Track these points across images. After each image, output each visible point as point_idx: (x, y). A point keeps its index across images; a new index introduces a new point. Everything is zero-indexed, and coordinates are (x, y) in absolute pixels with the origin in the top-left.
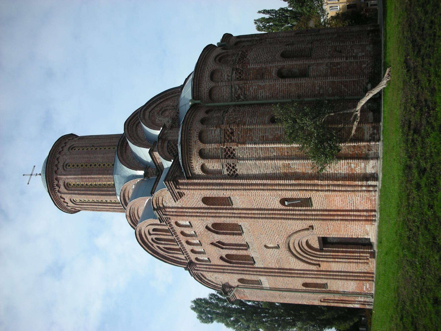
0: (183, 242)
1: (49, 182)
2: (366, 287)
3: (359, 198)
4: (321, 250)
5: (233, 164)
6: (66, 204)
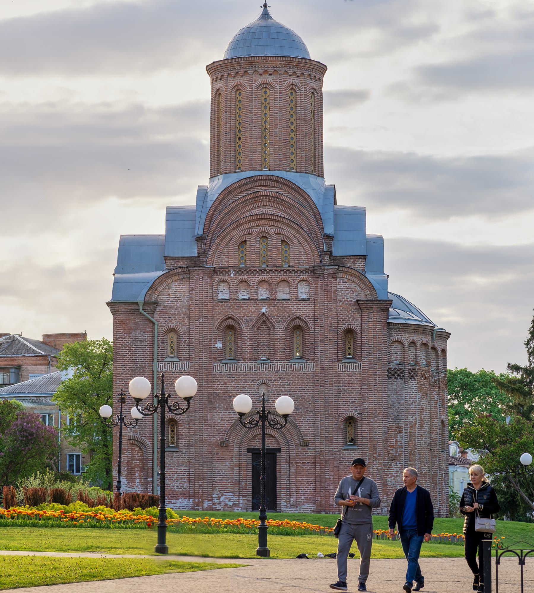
0: (265, 277)
1: (301, 63)
4: (249, 450)
5: (403, 376)
6: (261, 71)
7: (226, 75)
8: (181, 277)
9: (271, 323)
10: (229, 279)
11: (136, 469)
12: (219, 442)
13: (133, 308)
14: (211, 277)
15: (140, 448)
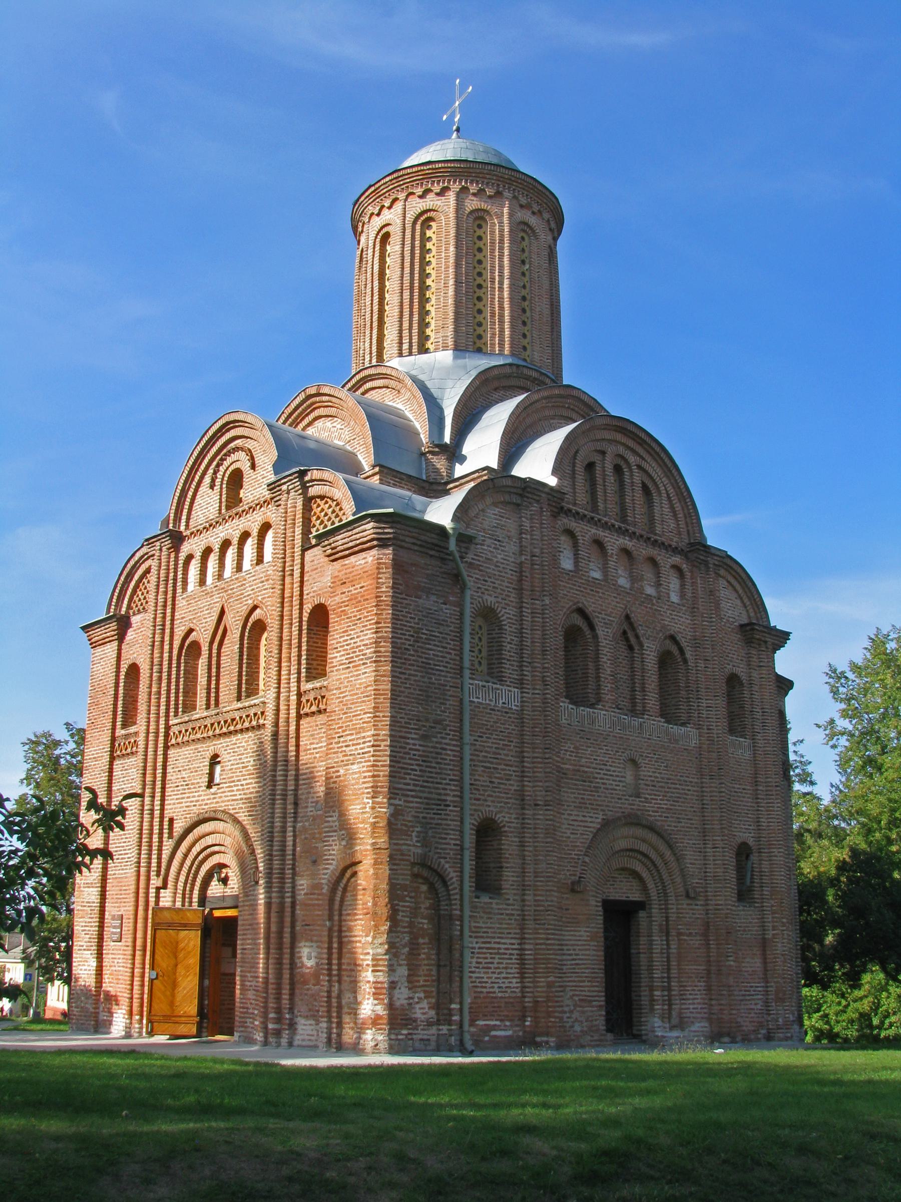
2: (495, 1028)
3: (759, 1007)
7: (456, 187)
8: (507, 498)
9: (637, 637)
10: (578, 529)
11: (421, 941)
12: (570, 881)
13: (429, 540)
14: (555, 516)
15: (432, 886)
